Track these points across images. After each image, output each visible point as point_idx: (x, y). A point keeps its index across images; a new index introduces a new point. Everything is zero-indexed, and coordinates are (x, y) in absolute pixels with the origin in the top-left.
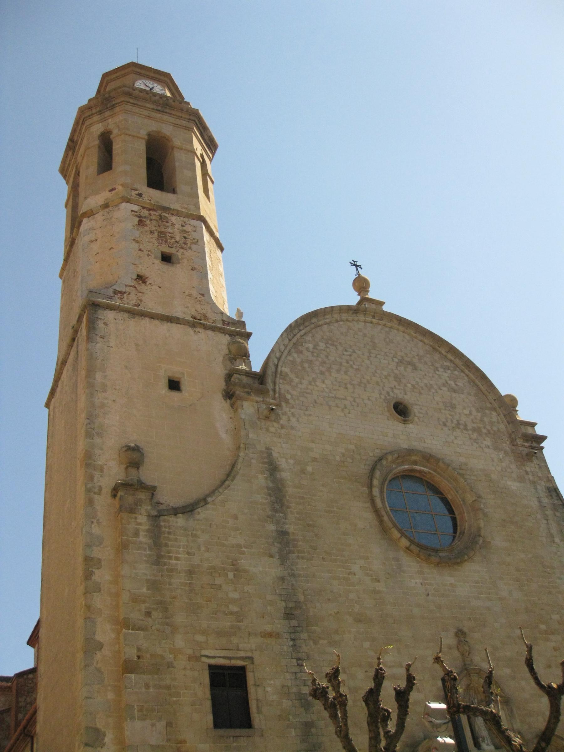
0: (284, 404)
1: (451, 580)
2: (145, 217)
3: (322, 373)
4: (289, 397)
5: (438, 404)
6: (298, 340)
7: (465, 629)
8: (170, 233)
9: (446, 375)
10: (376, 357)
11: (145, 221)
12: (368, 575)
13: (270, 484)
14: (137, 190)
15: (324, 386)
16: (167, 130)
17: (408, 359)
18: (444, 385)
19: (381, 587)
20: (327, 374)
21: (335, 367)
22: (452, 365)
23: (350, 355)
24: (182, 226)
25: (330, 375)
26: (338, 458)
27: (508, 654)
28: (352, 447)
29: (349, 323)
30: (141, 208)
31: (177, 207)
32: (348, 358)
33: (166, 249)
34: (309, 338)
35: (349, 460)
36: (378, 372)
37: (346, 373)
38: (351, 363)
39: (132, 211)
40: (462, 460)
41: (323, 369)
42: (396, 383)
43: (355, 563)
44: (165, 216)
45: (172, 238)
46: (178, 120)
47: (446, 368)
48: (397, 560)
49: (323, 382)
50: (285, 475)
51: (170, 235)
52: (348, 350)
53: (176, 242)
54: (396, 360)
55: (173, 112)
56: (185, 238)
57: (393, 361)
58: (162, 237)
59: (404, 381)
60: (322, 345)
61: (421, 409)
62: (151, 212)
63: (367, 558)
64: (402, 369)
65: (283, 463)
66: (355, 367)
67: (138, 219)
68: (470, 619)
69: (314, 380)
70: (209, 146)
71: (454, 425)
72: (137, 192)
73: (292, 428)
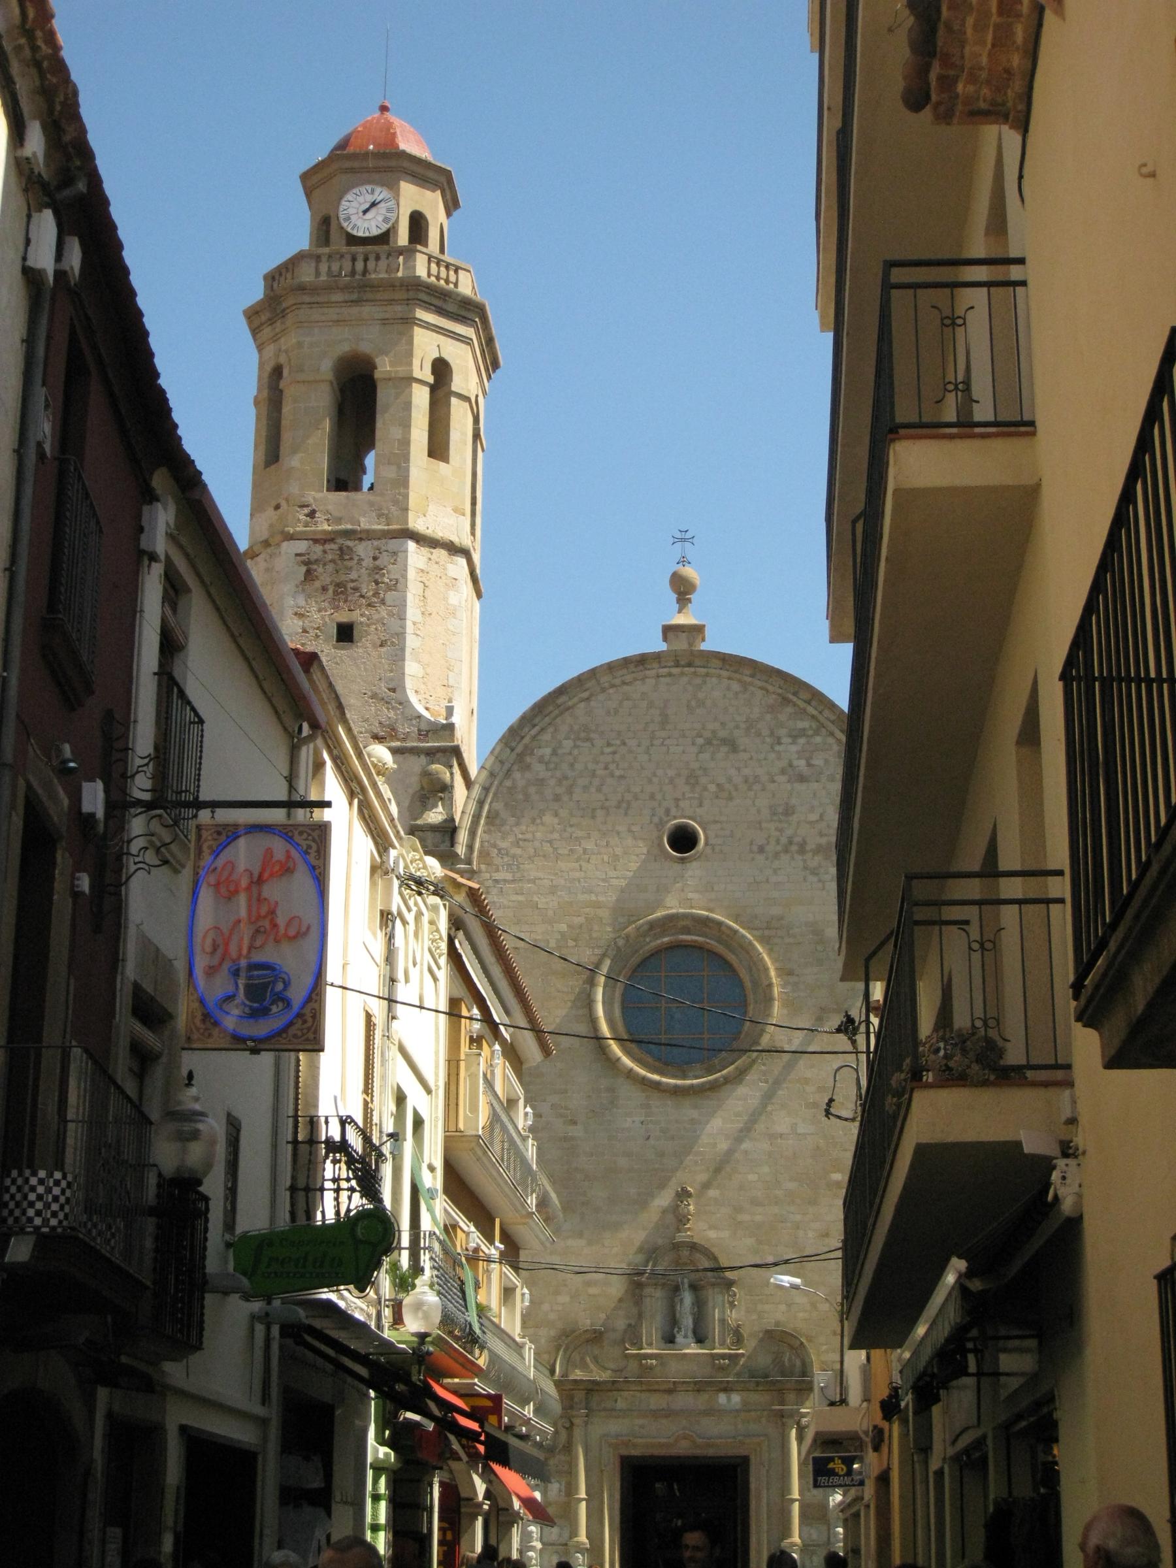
1: (694, 1114)
2: (317, 561)
3: (557, 798)
5: (759, 811)
6: (526, 747)
8: (353, 581)
9: (791, 750)
10: (662, 744)
11: (315, 570)
12: (561, 1116)
14: (307, 506)
15: (556, 820)
17: (722, 734)
18: (783, 772)
19: (577, 1131)
20: (565, 798)
21: (581, 782)
22: (814, 725)
23: (614, 753)
24: (375, 558)
25: (571, 800)
27: (758, 1218)
29: (626, 688)
30: (311, 542)
32: (609, 758)
33: (343, 617)
34: (547, 737)
35: (571, 943)
36: (660, 772)
37: (599, 790)
38: (612, 767)
39: (297, 555)
40: (776, 911)
41: (559, 790)
42: (687, 788)
43: (544, 1101)
44: (348, 547)
45: (356, 589)
46: (389, 308)
47: (795, 736)
48: (611, 1090)
49: (556, 815)
51: (352, 585)
52: (613, 742)
54: (700, 741)
55: (379, 296)
57: (693, 744)
59: (703, 780)
60: (568, 744)
61: (722, 829)
62: (328, 547)
63: (566, 1091)
64: (706, 756)
66: (617, 773)
67: (304, 569)
69: (542, 813)
70: (464, 317)
71: (779, 848)
72: (306, 511)
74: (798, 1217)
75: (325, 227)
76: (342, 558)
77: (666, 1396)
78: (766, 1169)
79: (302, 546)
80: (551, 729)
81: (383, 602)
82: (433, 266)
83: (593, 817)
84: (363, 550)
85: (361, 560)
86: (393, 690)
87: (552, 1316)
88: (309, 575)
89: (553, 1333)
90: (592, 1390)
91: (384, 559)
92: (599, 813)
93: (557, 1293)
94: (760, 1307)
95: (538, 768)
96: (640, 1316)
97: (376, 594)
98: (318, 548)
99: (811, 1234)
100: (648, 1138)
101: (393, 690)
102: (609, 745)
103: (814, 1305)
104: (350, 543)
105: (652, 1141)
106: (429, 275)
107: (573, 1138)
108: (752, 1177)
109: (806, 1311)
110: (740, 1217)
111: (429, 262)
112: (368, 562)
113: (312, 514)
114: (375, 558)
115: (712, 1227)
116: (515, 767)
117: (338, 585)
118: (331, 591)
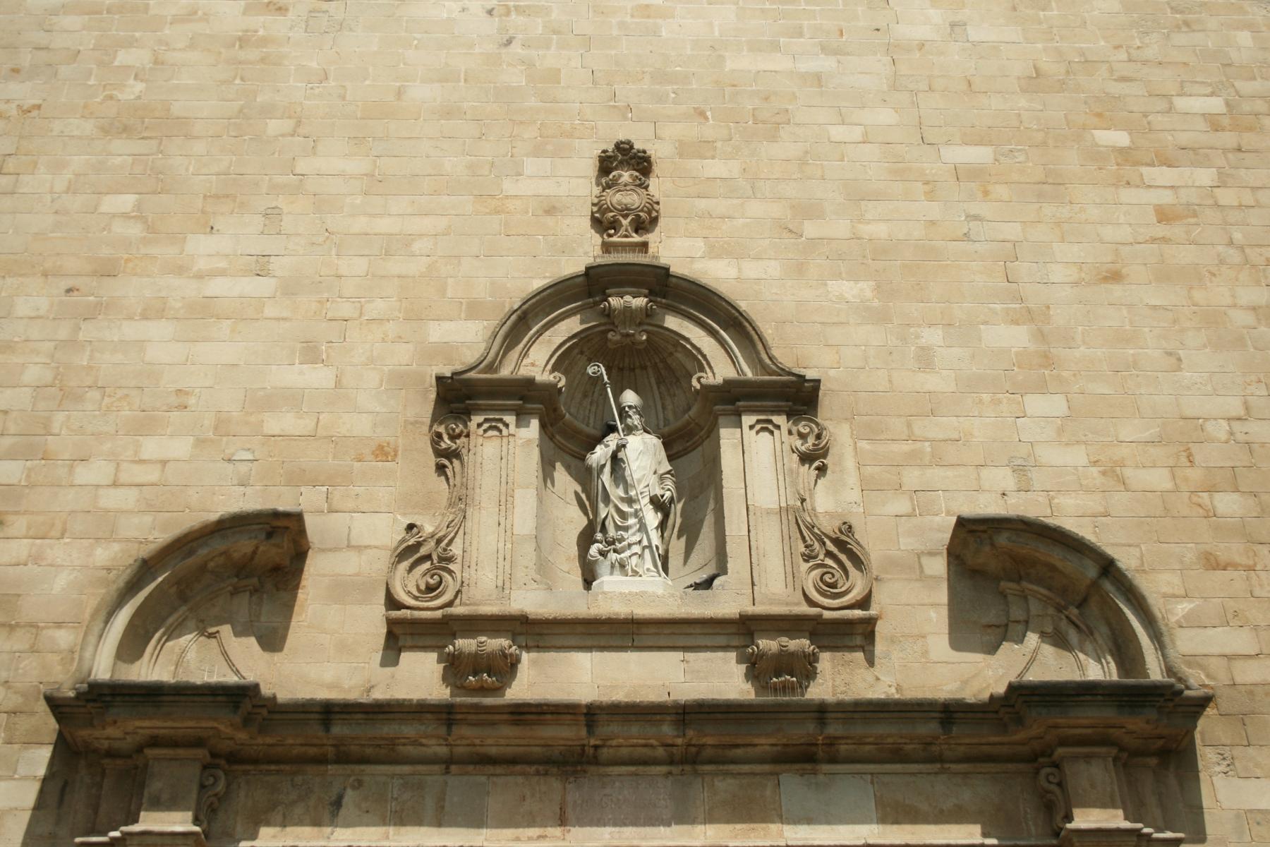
7: (656, 151)
27: (880, 230)
68: (702, 114)
74: (1012, 231)
77: (556, 784)
78: (885, 116)
87: (112, 499)
89: (104, 554)
90: (234, 758)
93: (146, 425)
94: (912, 477)
96: (461, 501)
99: (1058, 273)
100: (509, 42)
103: (1114, 473)
105: (516, 48)
107: (264, 41)
108: (838, 132)
109: (1088, 491)
110: (811, 229)
115: (715, 252)
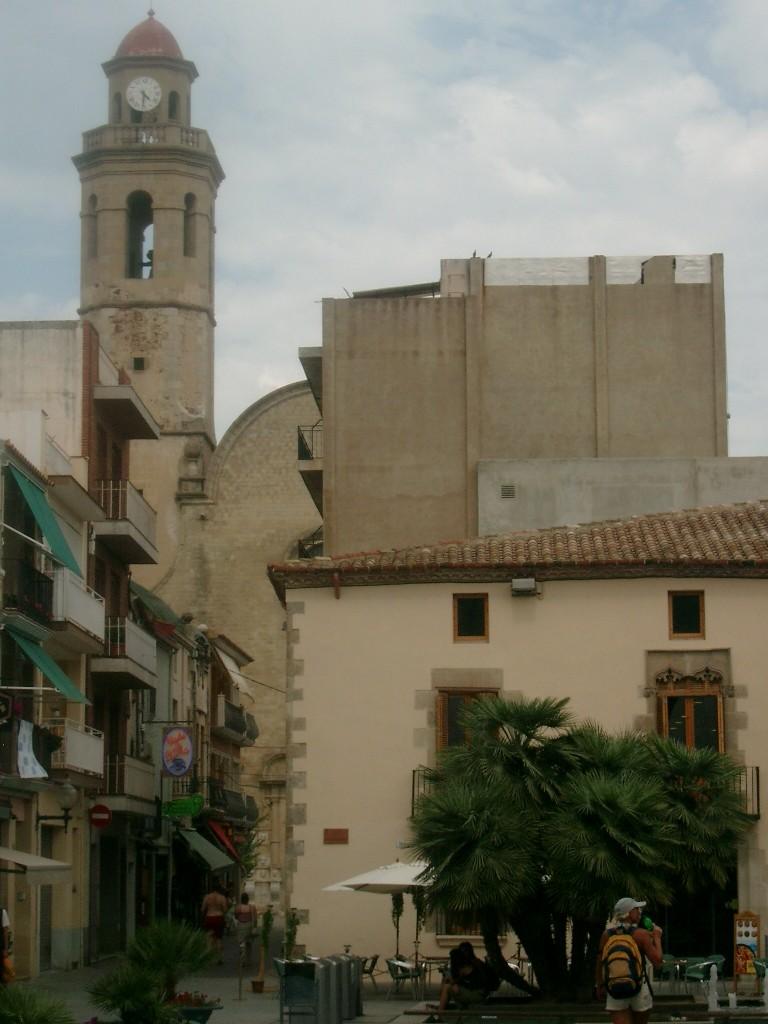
0: (220, 502)
2: (121, 322)
4: (225, 493)
6: (242, 433)
13: (199, 576)
16: (147, 184)
24: (155, 320)
26: (259, 544)
28: (273, 531)
29: (299, 399)
31: (152, 297)
33: (138, 355)
34: (253, 427)
50: (212, 566)
53: (148, 342)
56: (156, 334)
58: (136, 339)
62: (128, 312)
65: (211, 556)
67: (114, 325)
72: (114, 290)
73: (224, 523)
75: (118, 100)
76: (136, 318)
79: (111, 312)
80: (256, 423)
81: (160, 346)
82: (184, 133)
83: (281, 473)
84: (148, 314)
85: (147, 321)
86: (167, 398)
88: (118, 330)
91: (161, 320)
92: (284, 471)
95: (249, 445)
97: (156, 342)
98: (123, 313)
101: (167, 398)
102: (289, 432)
104: (140, 310)
106: (182, 140)
111: (182, 131)
112: (151, 321)
113: (118, 292)
114: (155, 320)
116: (237, 445)
117: (134, 336)
118: (131, 337)
